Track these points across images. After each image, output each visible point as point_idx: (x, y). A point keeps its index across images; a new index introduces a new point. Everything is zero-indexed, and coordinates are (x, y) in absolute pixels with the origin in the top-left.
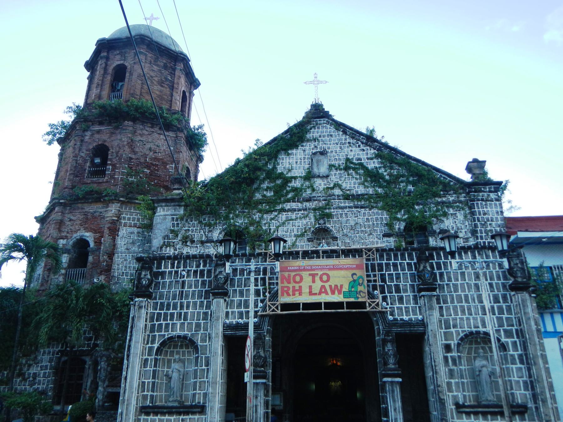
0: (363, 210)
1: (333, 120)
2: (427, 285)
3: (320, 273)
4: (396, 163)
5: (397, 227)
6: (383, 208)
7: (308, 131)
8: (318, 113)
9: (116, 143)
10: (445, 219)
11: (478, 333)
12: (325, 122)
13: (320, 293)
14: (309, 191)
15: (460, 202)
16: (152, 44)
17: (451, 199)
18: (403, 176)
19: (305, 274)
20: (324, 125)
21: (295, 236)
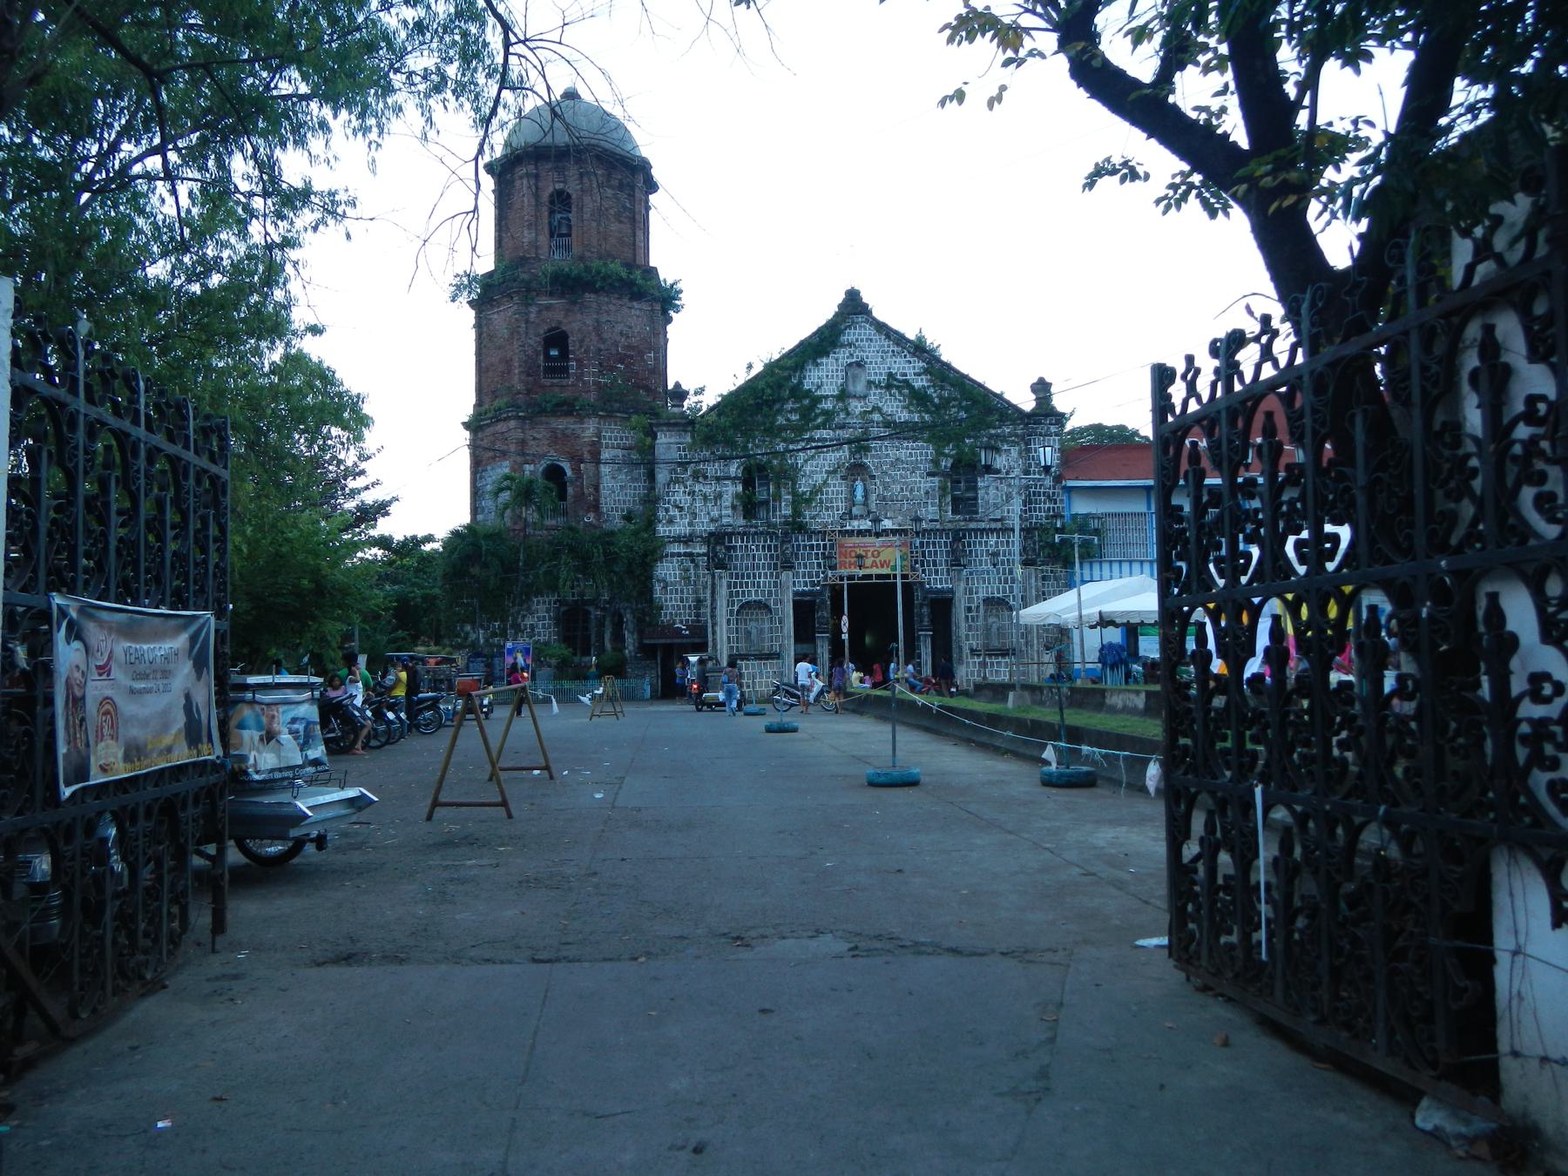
2: (957, 560)
7: (842, 332)
8: (854, 306)
9: (576, 326)
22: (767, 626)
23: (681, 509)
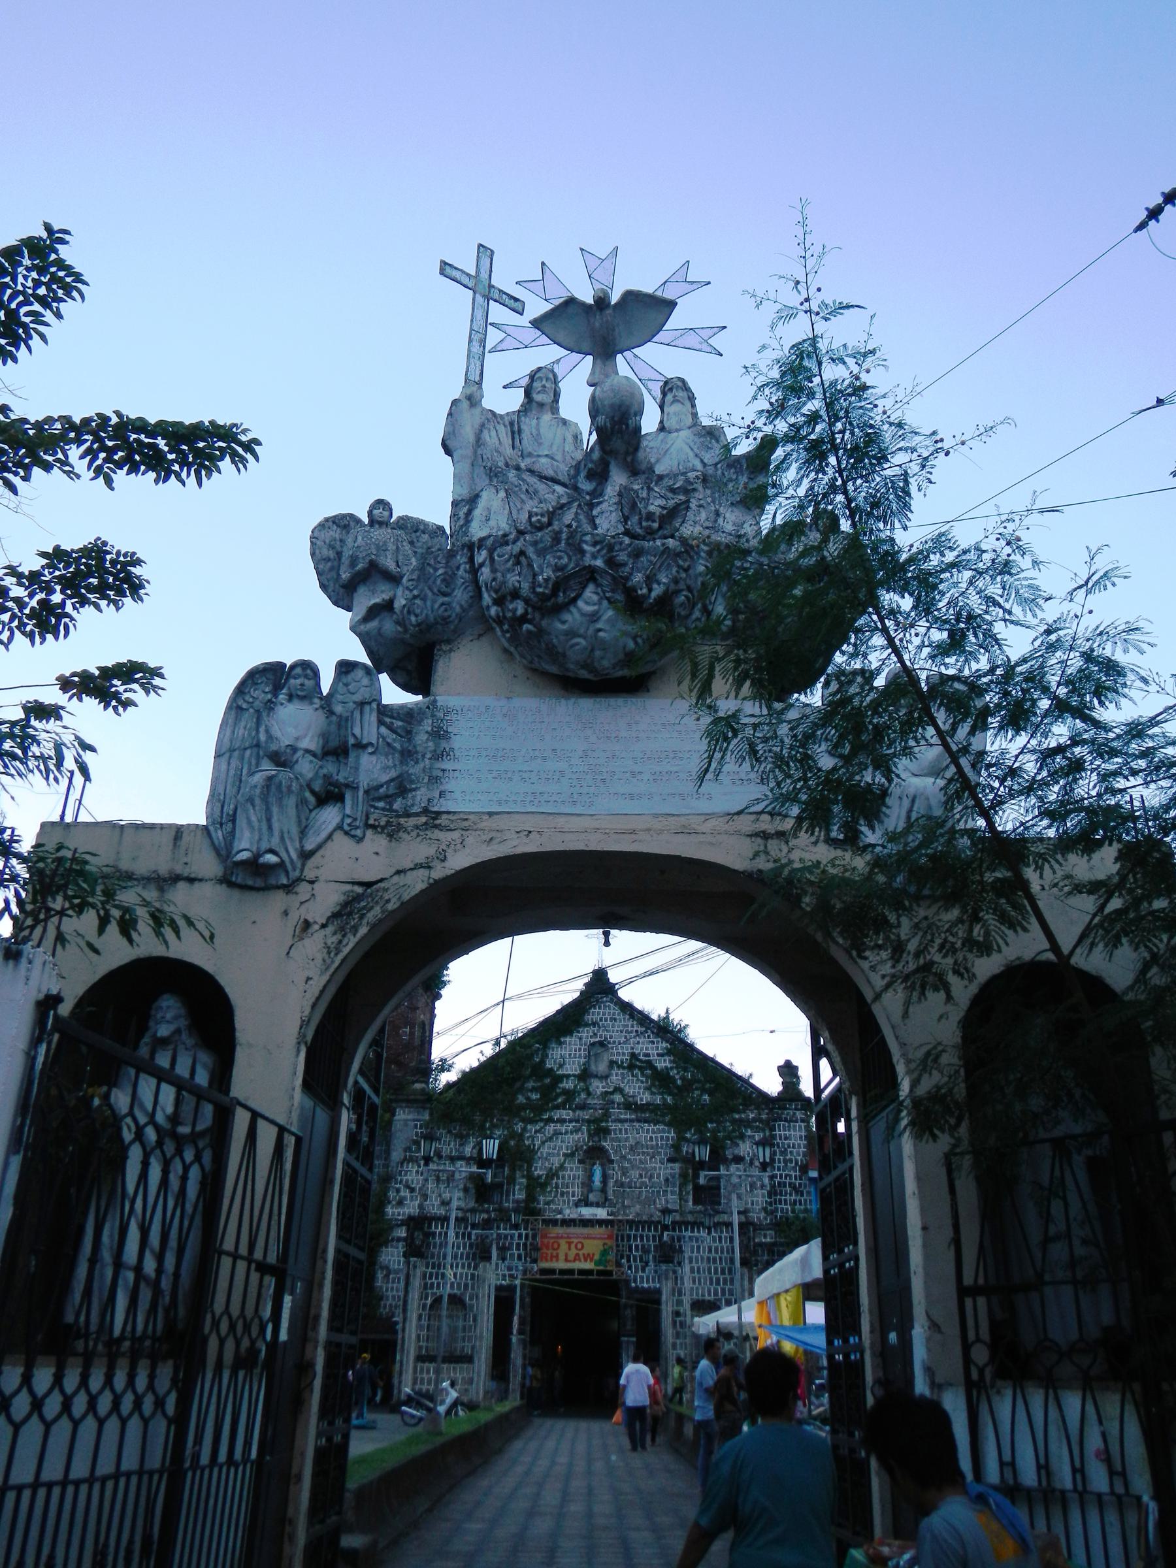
1: (619, 999)
3: (575, 1241)
6: (669, 1124)
7: (586, 1012)
10: (740, 1142)
11: (703, 1301)
13: (574, 1261)
14: (583, 1096)
15: (761, 1121)
17: (751, 1116)
18: (698, 1081)
19: (563, 1242)
21: (564, 1155)
22: (461, 1323)
23: (412, 1190)
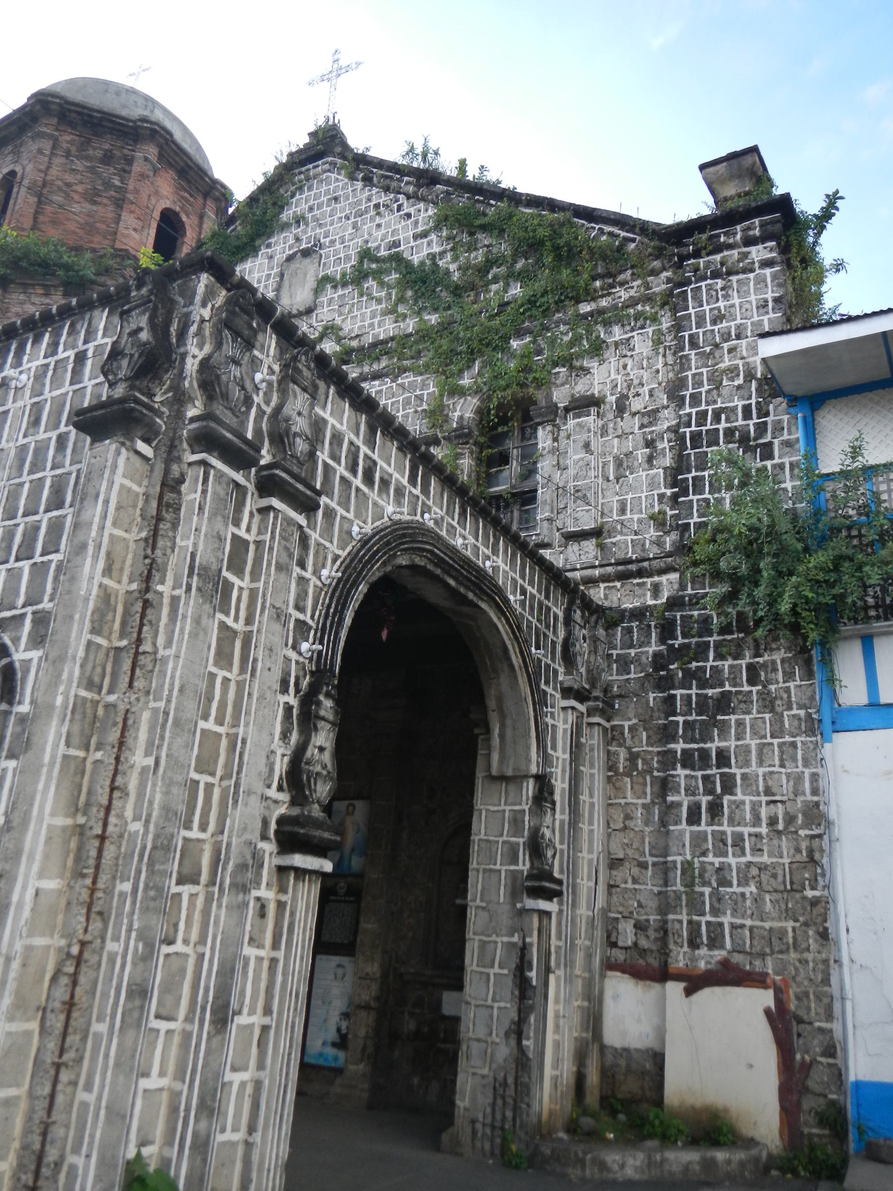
0: (377, 383)
4: (484, 228)
5: (457, 414)
10: (591, 363)
12: (327, 166)
16: (70, 111)
17: (623, 295)
20: (324, 176)
